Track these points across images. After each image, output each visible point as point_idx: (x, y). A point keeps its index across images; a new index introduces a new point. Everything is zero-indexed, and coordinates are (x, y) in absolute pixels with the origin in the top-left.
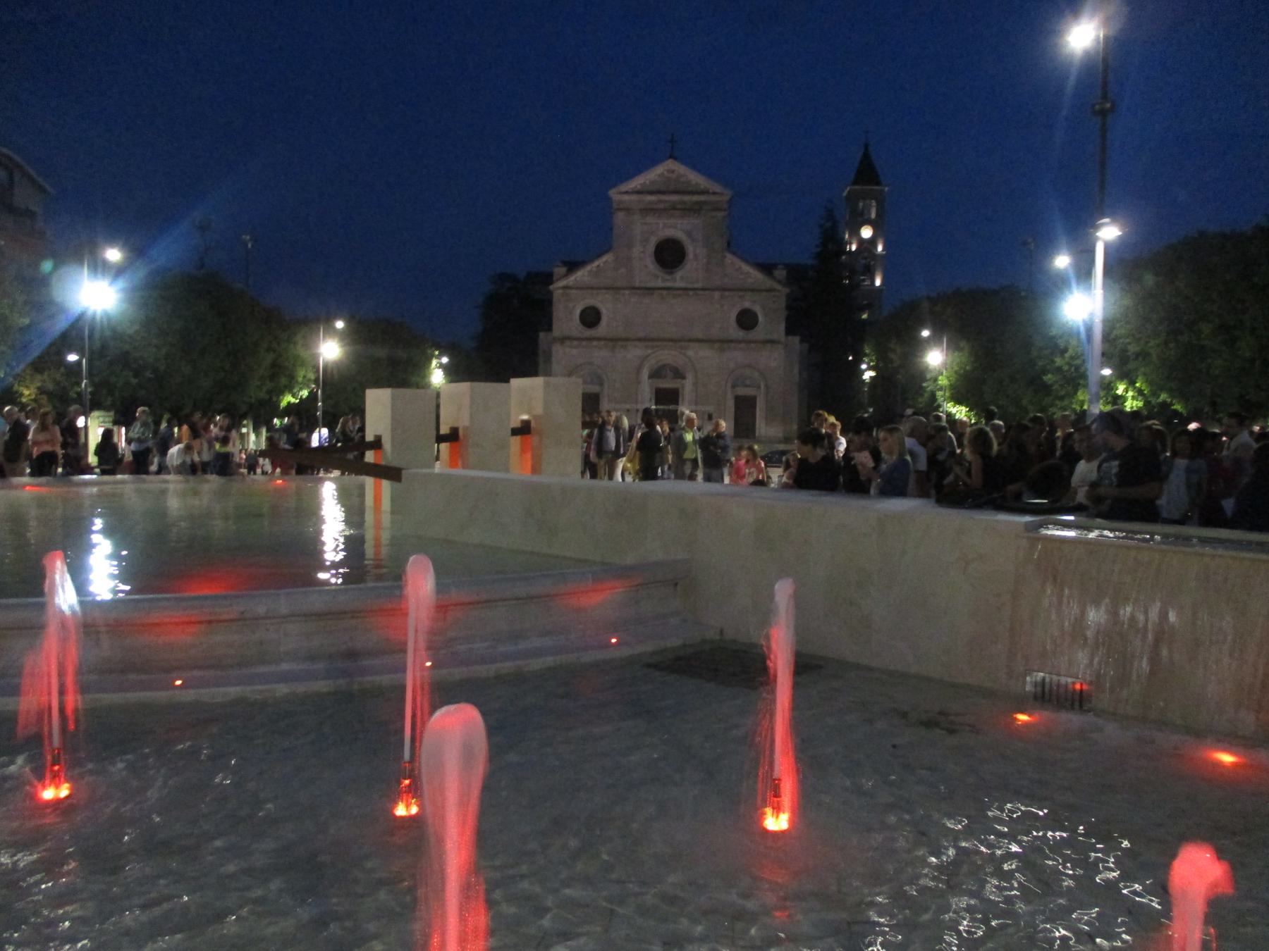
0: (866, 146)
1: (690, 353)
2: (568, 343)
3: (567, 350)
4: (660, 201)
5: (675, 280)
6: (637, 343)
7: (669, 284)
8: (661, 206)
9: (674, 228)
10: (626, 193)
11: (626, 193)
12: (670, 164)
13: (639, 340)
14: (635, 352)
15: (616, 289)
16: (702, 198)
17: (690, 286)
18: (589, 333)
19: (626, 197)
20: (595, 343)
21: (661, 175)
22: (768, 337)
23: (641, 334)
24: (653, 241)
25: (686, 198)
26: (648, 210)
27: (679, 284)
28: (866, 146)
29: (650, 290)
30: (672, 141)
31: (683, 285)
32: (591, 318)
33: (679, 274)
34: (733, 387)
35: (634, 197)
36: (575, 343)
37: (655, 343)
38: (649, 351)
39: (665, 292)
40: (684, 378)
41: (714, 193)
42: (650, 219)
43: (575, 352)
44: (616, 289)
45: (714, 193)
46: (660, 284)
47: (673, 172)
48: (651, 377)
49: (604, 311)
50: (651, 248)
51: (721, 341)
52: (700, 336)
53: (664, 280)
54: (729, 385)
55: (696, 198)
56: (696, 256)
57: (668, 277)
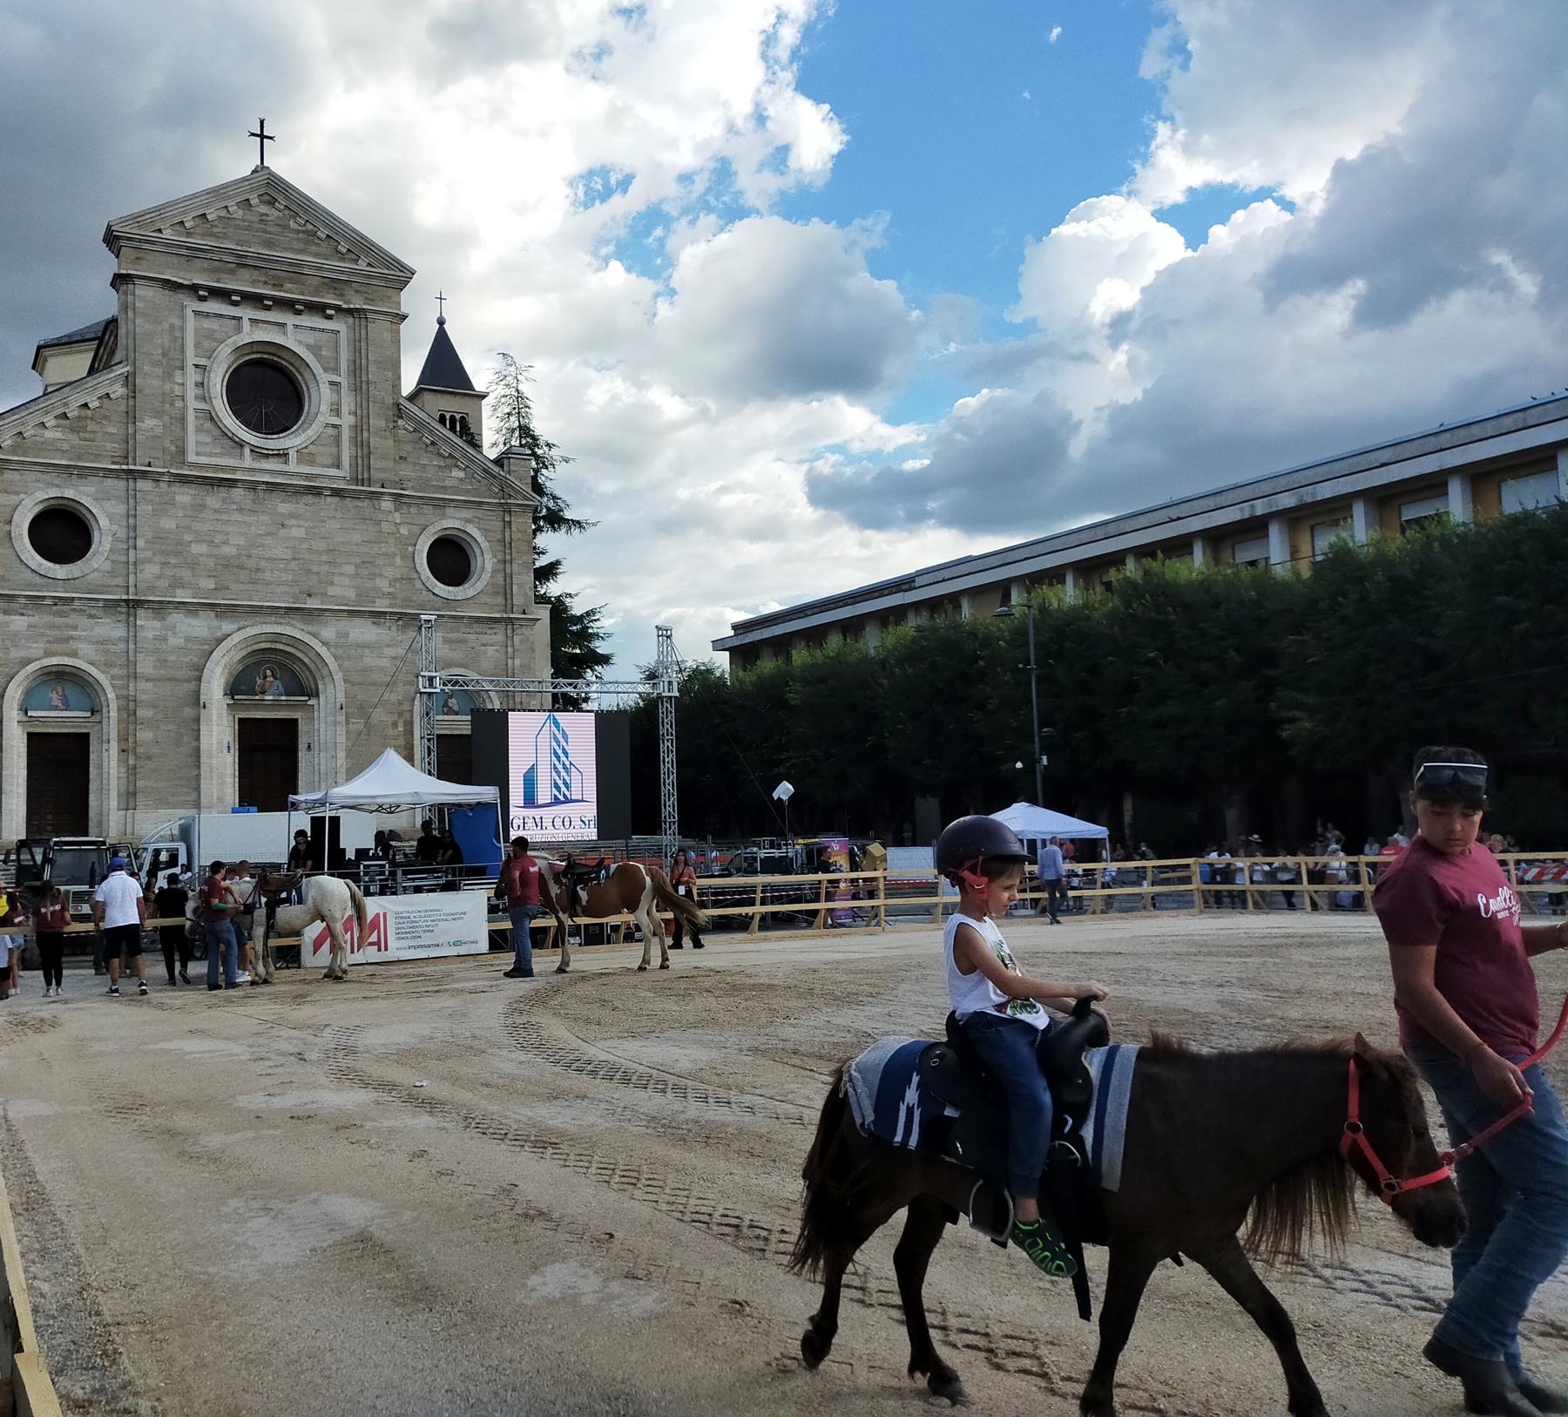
27: (293, 466)
38: (227, 626)
40: (315, 694)
42: (213, 306)
48: (233, 690)
50: (218, 382)
53: (258, 453)
56: (336, 411)
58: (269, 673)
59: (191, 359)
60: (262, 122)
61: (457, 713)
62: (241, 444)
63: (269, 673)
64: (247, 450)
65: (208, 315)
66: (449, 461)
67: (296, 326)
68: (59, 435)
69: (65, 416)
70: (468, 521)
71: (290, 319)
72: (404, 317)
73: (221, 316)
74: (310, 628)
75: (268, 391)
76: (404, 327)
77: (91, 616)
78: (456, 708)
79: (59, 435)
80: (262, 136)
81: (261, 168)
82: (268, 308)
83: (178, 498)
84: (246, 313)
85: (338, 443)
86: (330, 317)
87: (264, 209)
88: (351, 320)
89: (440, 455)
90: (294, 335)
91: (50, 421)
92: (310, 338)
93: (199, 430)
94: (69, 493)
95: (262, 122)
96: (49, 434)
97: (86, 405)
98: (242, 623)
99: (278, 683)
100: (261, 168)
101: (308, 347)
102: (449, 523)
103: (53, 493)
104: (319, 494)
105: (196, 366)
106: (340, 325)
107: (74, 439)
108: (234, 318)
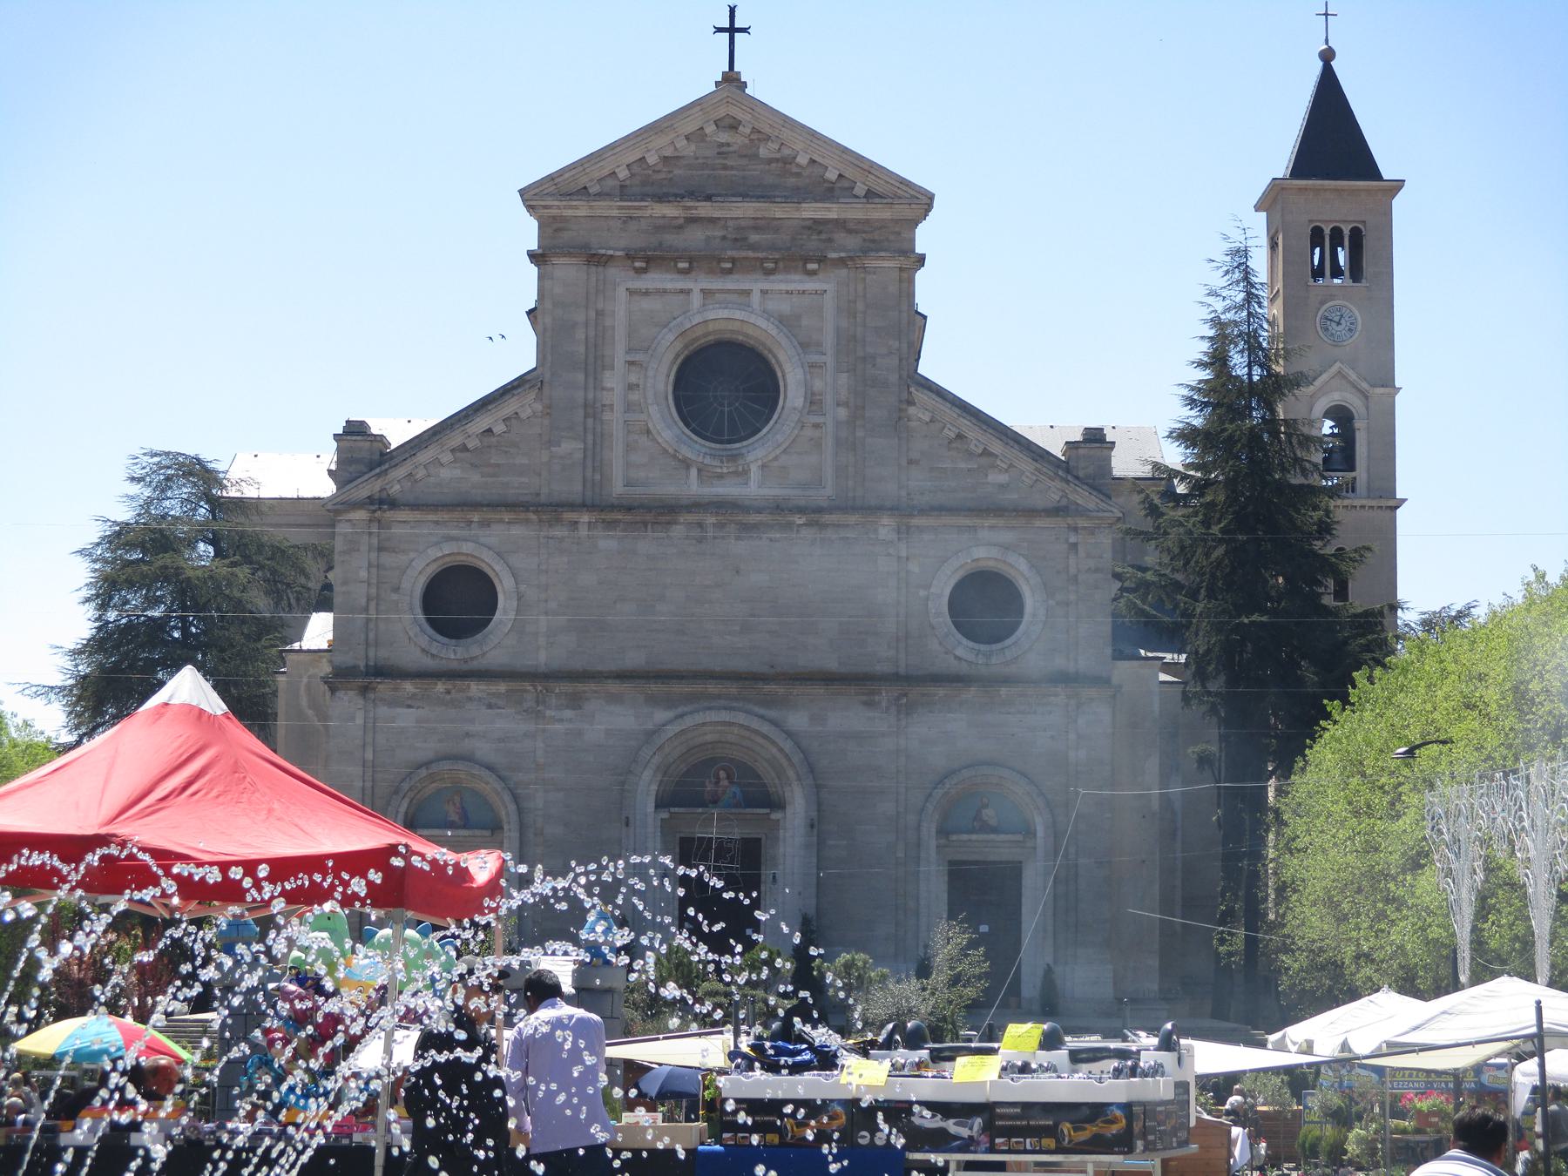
0: (1327, 56)
1: (798, 720)
2: (384, 687)
3: (383, 711)
6: (613, 687)
7: (728, 490)
8: (695, 237)
13: (622, 676)
14: (612, 721)
15: (550, 510)
16: (831, 211)
18: (453, 653)
20: (475, 688)
22: (1060, 662)
23: (634, 659)
27: (754, 488)
28: (1327, 56)
29: (662, 512)
30: (732, 30)
31: (772, 491)
32: (458, 600)
33: (757, 452)
34: (943, 832)
36: (409, 687)
37: (679, 688)
38: (661, 715)
40: (780, 805)
42: (656, 279)
43: (406, 718)
44: (550, 510)
46: (693, 487)
49: (505, 586)
51: (895, 678)
52: (832, 664)
54: (929, 829)
55: (811, 211)
56: (814, 402)
58: (722, 774)
59: (620, 355)
60: (732, 11)
61: (995, 830)
62: (686, 464)
63: (722, 774)
64: (694, 472)
65: (647, 293)
66: (984, 461)
67: (764, 292)
68: (457, 473)
69: (464, 448)
70: (1006, 548)
71: (756, 284)
72: (921, 260)
73: (665, 291)
74: (772, 714)
75: (725, 387)
76: (920, 277)
77: (490, 706)
78: (993, 822)
79: (457, 473)
80: (732, 30)
81: (731, 79)
82: (730, 271)
83: (602, 544)
84: (698, 283)
85: (818, 444)
86: (813, 273)
87: (724, 137)
88: (844, 272)
89: (970, 455)
90: (753, 308)
91: (447, 457)
92: (785, 307)
93: (629, 448)
94: (467, 548)
95: (732, 11)
96: (445, 473)
97: (489, 431)
98: (680, 710)
99: (735, 789)
100: (731, 79)
101: (783, 321)
102: (980, 553)
103: (447, 549)
104: (789, 526)
105: (631, 363)
106: (826, 285)
107: (476, 478)
108: (682, 291)
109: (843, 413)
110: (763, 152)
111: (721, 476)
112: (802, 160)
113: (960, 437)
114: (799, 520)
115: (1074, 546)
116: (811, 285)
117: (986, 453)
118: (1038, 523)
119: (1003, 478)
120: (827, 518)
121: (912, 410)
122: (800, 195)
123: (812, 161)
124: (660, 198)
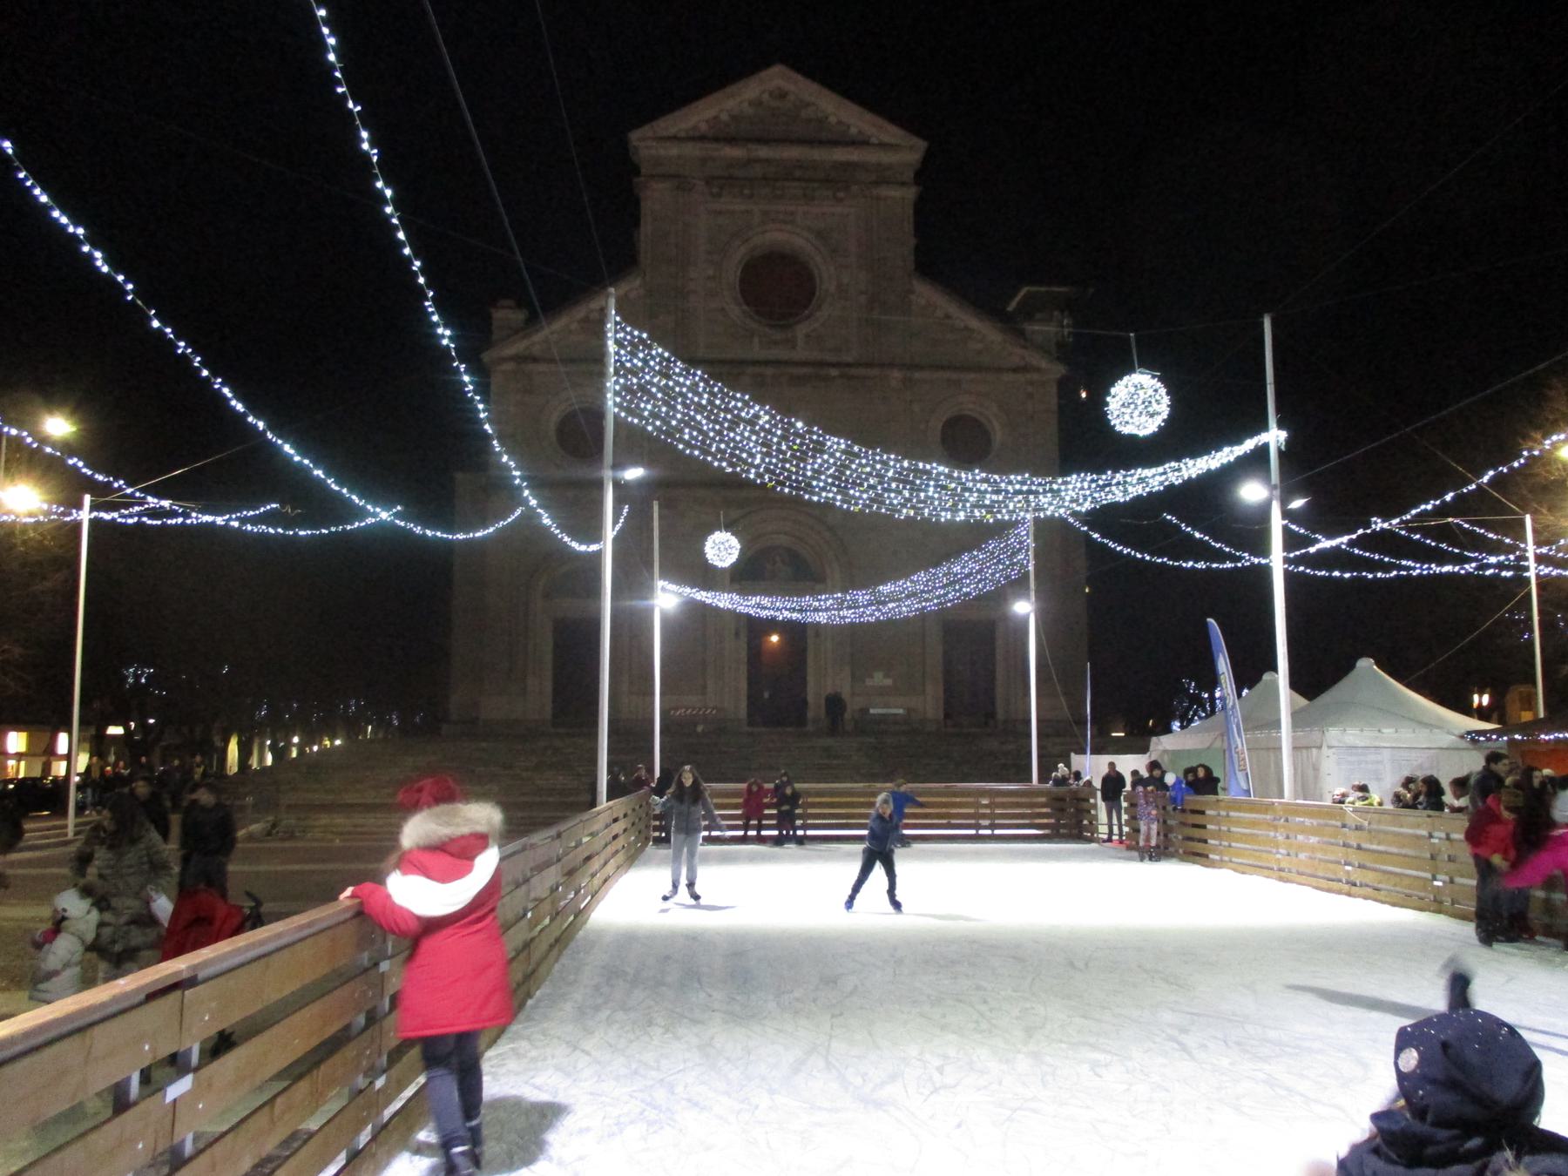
4: (750, 162)
5: (791, 343)
9: (790, 228)
10: (675, 138)
11: (675, 138)
12: (777, 78)
16: (854, 155)
17: (829, 358)
19: (674, 150)
21: (757, 103)
24: (739, 254)
25: (818, 154)
26: (725, 181)
27: (800, 353)
31: (815, 355)
33: (801, 330)
35: (692, 150)
39: (769, 371)
41: (882, 146)
45: (882, 146)
46: (757, 351)
47: (783, 95)
55: (840, 155)
57: (778, 335)
64: (756, 340)
86: (841, 200)
109: (863, 299)
110: (804, 114)
111: (776, 343)
112: (833, 119)
113: (948, 317)
114: (834, 372)
115: (1030, 396)
116: (839, 209)
117: (966, 328)
118: (1008, 377)
119: (979, 346)
120: (853, 371)
121: (913, 297)
122: (835, 143)
123: (840, 122)
124: (731, 140)
